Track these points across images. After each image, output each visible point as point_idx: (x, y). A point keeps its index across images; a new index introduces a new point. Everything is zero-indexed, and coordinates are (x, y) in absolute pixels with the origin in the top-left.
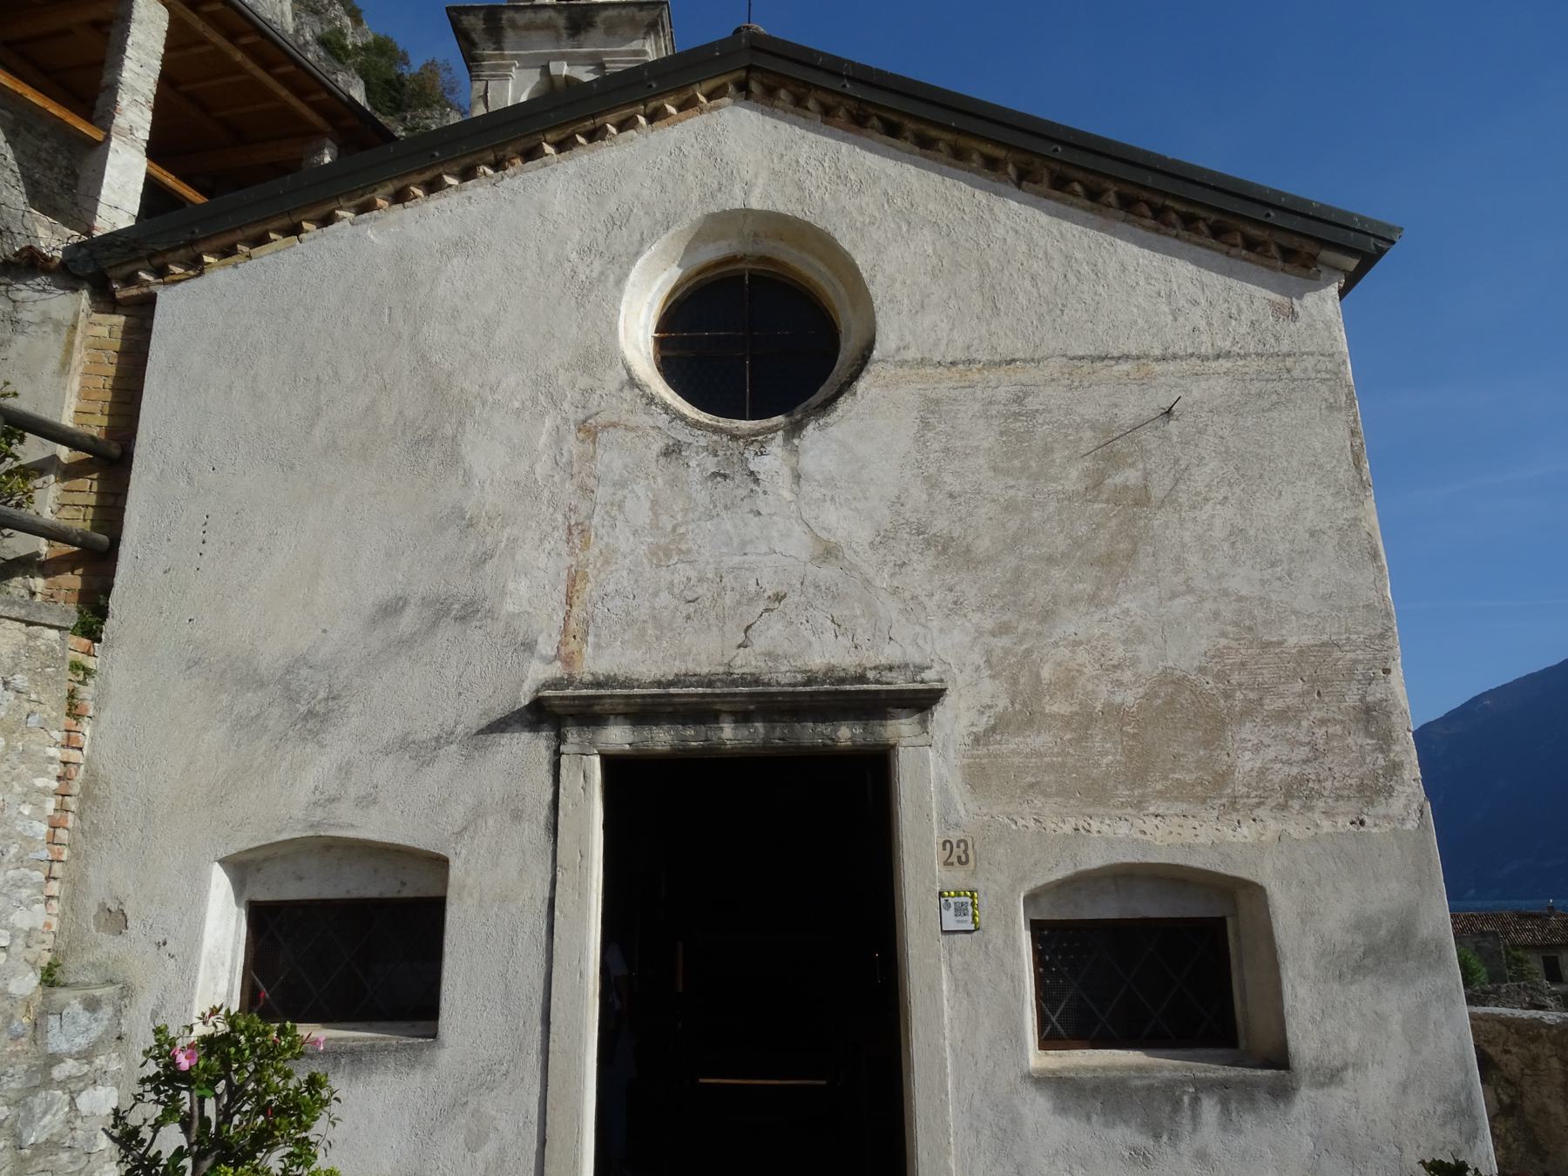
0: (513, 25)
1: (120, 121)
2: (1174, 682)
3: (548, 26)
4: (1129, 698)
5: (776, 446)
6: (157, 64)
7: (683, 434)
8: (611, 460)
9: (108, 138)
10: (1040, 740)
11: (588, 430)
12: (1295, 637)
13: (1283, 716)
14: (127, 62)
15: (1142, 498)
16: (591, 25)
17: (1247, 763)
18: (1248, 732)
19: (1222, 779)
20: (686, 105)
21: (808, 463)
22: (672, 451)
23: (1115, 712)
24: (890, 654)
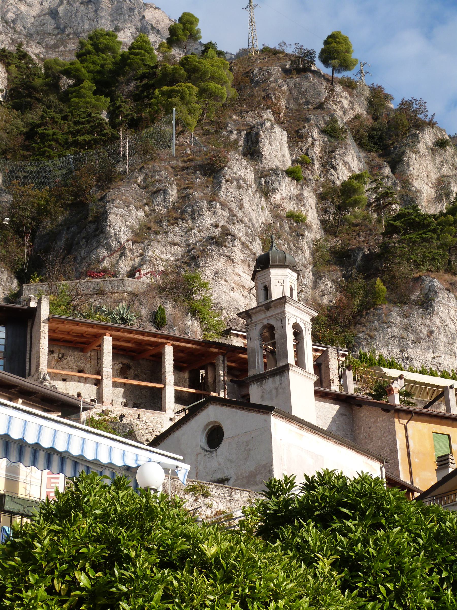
0: (253, 313)
1: (167, 381)
2: (252, 472)
3: (260, 311)
4: (247, 475)
5: (214, 452)
6: (172, 362)
7: (205, 453)
8: (199, 458)
9: (165, 386)
10: (239, 482)
11: (197, 455)
12: (264, 463)
13: (262, 473)
14: (166, 366)
15: (250, 450)
16: (270, 307)
17: (258, 479)
18: (258, 476)
19: (255, 482)
20: (205, 408)
21: (218, 454)
22: (205, 455)
23: (246, 476)
24: (225, 475)
